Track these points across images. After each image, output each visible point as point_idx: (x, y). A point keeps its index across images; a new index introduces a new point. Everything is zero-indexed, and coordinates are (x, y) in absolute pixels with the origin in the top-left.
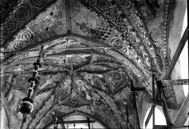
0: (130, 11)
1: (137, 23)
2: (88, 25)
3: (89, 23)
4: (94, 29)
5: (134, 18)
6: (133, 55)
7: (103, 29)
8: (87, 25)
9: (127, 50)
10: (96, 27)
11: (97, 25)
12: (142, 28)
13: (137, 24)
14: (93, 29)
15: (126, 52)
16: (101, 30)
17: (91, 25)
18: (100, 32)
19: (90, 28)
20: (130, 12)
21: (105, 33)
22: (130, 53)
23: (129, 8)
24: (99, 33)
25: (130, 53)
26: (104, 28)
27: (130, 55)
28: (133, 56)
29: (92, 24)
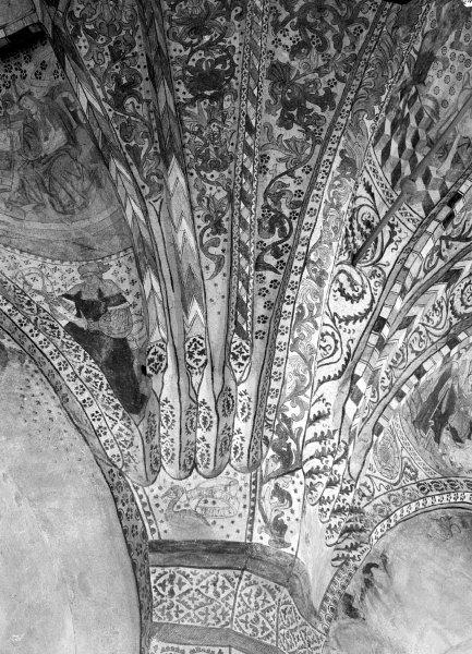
0: (445, 309)
1: (416, 348)
2: (452, 46)
3: (458, 53)
4: (426, 82)
5: (428, 331)
6: (336, 342)
7: (416, 140)
8: (452, 38)
9: (348, 297)
10: (431, 92)
11: (435, 101)
12: (416, 386)
13: (413, 351)
14: (431, 72)
15: (342, 291)
16: (413, 122)
17: (445, 61)
18: (407, 110)
19: (439, 54)
20: (442, 309)
21: (402, 147)
22: (340, 321)
23: (452, 302)
24: (404, 108)
25: (343, 324)
26: (418, 146)
27: (333, 321)
28: (330, 340)
29: (446, 73)
